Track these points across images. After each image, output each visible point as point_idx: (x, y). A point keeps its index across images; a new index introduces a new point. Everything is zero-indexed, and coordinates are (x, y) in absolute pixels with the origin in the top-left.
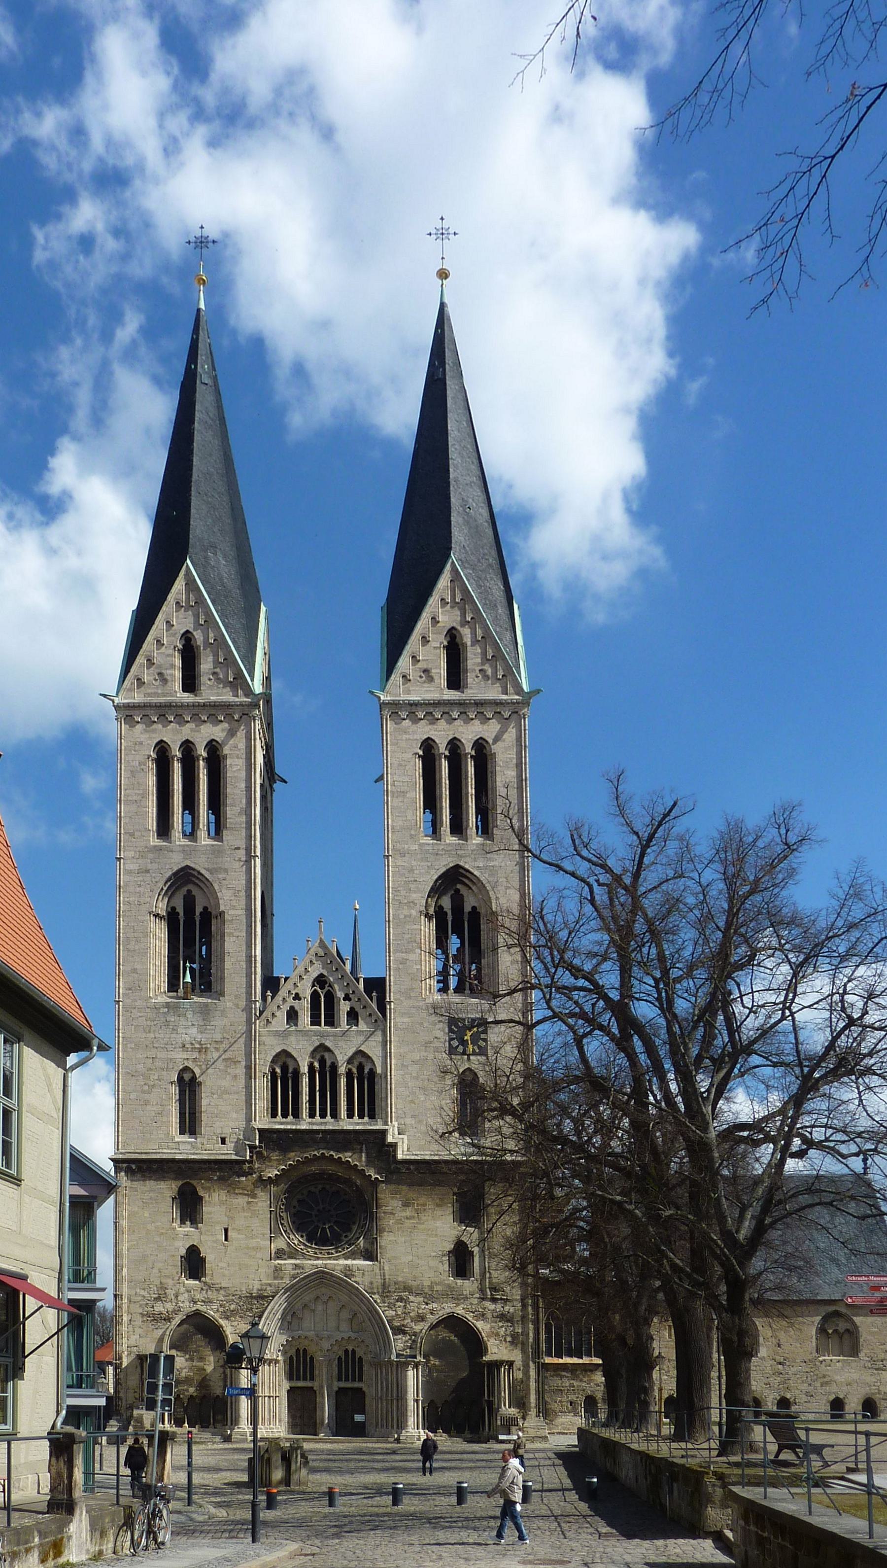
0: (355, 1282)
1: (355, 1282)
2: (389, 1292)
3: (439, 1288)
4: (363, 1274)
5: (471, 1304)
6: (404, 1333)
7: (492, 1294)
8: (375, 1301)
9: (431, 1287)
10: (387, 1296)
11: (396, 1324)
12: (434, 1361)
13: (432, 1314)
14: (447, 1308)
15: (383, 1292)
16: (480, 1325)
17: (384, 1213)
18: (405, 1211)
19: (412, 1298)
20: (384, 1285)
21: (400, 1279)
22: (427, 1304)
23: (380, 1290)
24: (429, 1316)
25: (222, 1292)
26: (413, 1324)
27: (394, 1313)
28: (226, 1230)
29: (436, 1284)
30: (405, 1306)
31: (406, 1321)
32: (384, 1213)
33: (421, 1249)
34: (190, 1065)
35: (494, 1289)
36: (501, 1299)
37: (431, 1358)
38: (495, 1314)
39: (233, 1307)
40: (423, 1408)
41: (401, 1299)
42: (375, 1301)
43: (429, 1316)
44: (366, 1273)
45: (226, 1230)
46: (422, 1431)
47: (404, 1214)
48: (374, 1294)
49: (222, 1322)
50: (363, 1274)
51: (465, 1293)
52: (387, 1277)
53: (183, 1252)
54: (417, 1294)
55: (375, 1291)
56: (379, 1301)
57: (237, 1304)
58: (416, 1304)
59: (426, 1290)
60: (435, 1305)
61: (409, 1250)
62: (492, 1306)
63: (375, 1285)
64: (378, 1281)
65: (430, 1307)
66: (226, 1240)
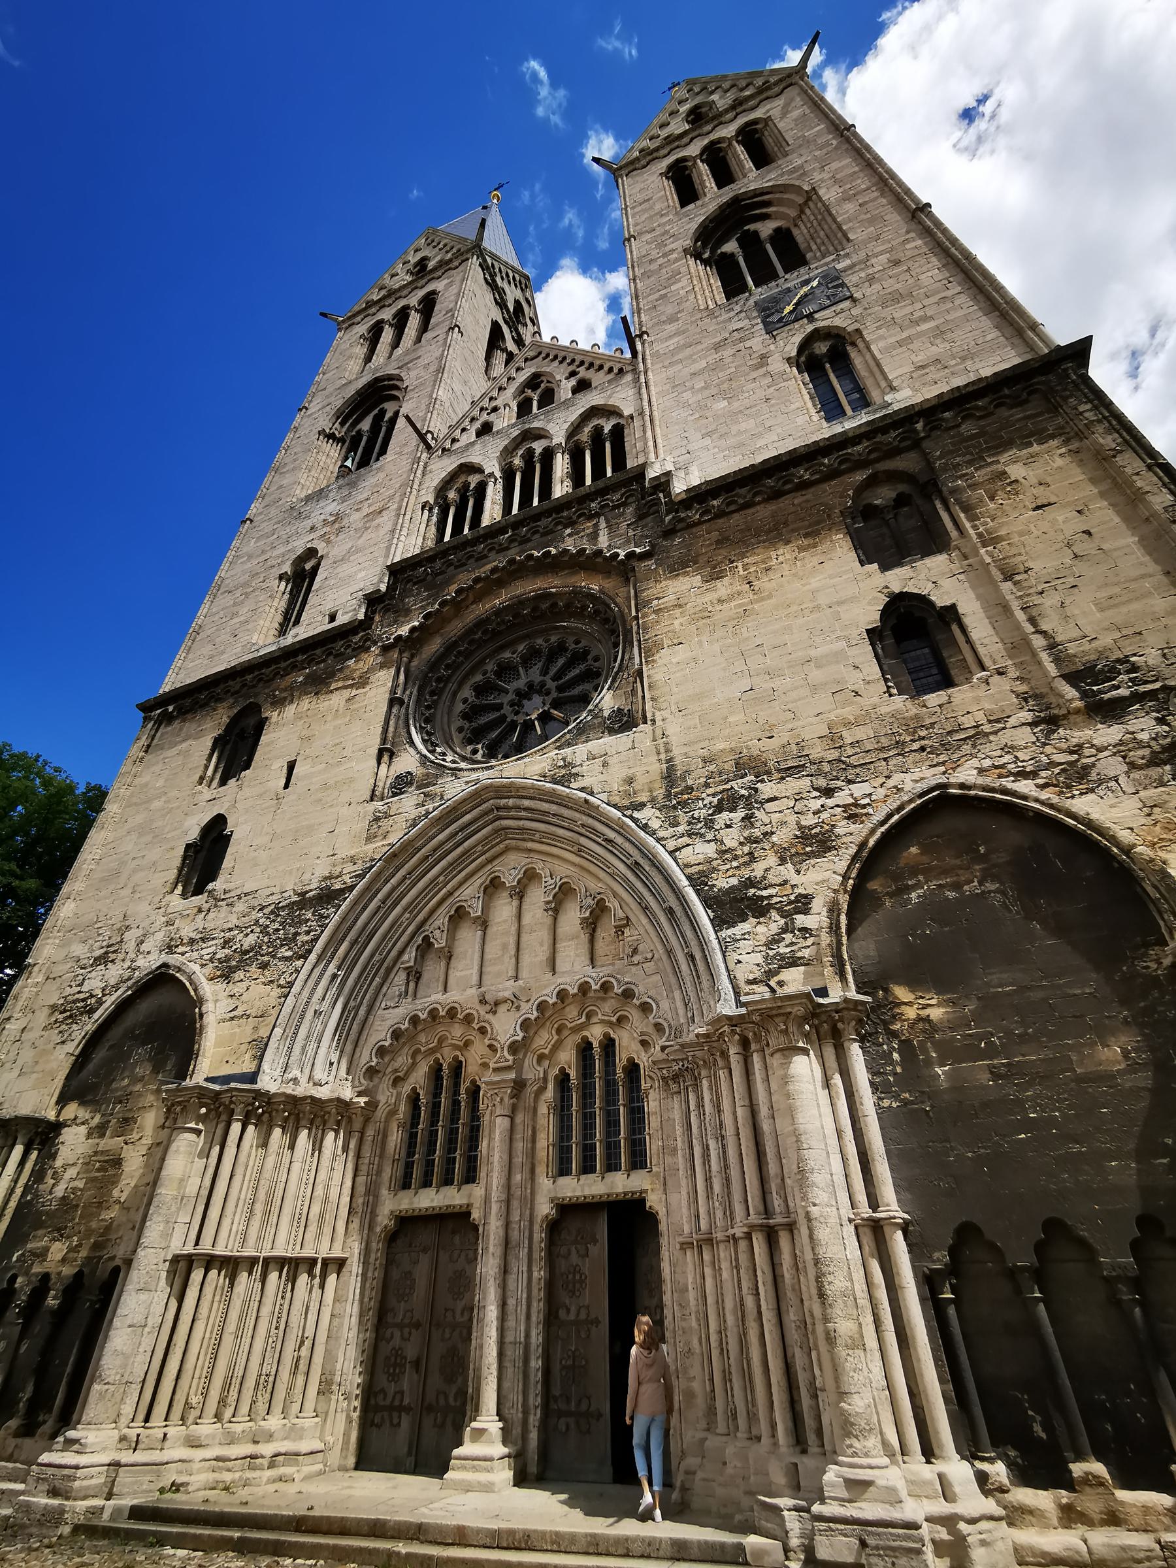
0: (582, 789)
1: (582, 789)
2: (689, 789)
3: (860, 733)
4: (605, 764)
5: (1008, 749)
6: (760, 909)
7: (1084, 695)
8: (645, 828)
9: (833, 738)
10: (683, 804)
11: (723, 882)
12: (920, 1006)
13: (852, 817)
14: (916, 779)
15: (668, 796)
16: (1085, 805)
17: (657, 612)
18: (714, 589)
19: (767, 789)
20: (670, 777)
21: (721, 745)
22: (828, 792)
23: (660, 792)
24: (843, 827)
25: (240, 907)
26: (788, 872)
27: (710, 850)
28: (291, 766)
29: (849, 724)
30: (748, 819)
31: (758, 870)
32: (657, 612)
33: (776, 652)
34: (315, 544)
35: (1083, 675)
36: (1137, 697)
37: (902, 993)
38: (1137, 755)
39: (251, 940)
40: (929, 1283)
41: (729, 802)
42: (645, 828)
43: (843, 827)
44: (612, 761)
45: (291, 766)
46: (959, 1470)
47: (711, 596)
48: (642, 805)
49: (208, 989)
50: (605, 764)
51: (968, 722)
52: (676, 752)
53: (193, 834)
54: (787, 773)
55: (643, 797)
56: (655, 824)
57: (264, 930)
58: (787, 807)
59: (816, 752)
60: (858, 790)
61: (739, 666)
62: (1109, 734)
63: (641, 782)
64: (649, 770)
65: (843, 797)
66: (286, 786)
